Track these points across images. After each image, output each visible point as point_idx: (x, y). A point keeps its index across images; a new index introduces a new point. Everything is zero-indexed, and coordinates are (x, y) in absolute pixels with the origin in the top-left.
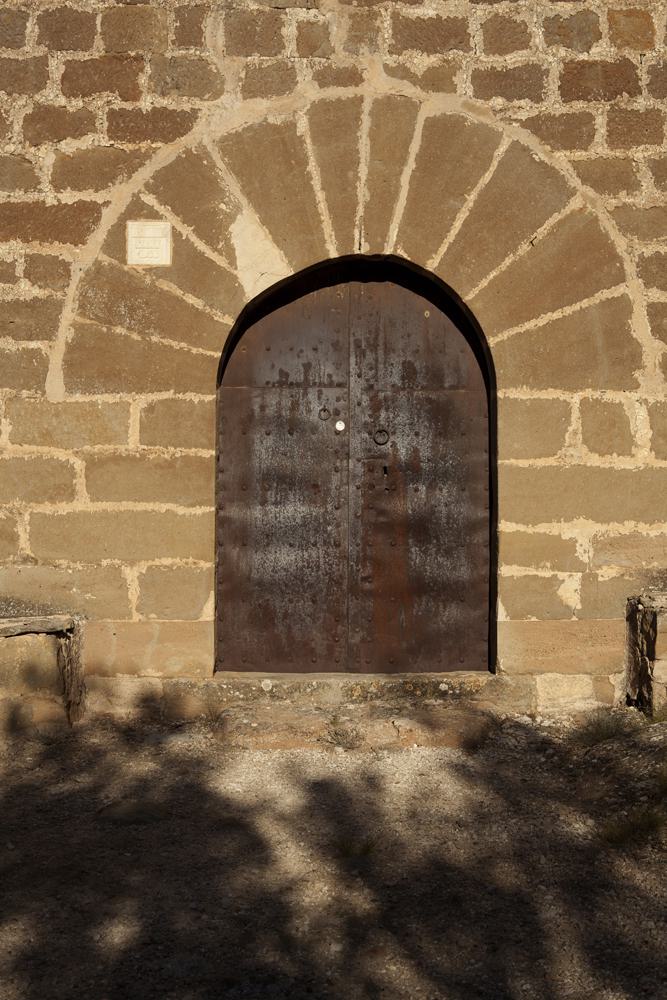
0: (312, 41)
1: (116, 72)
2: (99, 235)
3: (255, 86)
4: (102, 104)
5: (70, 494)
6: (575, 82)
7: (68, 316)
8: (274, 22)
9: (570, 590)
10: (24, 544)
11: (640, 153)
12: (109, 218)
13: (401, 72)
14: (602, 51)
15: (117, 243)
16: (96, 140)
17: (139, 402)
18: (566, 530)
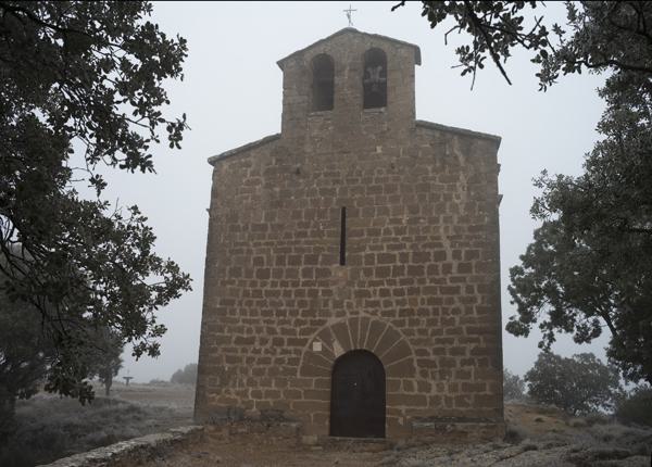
0: (350, 305)
1: (311, 313)
2: (308, 345)
3: (338, 315)
4: (309, 318)
5: (300, 397)
6: (402, 313)
7: (301, 361)
8: (342, 302)
9: (401, 421)
10: (292, 408)
11: (415, 328)
12: (310, 341)
13: (367, 312)
14: (407, 307)
15: (311, 346)
16: (308, 325)
17: (314, 379)
18: (398, 407)
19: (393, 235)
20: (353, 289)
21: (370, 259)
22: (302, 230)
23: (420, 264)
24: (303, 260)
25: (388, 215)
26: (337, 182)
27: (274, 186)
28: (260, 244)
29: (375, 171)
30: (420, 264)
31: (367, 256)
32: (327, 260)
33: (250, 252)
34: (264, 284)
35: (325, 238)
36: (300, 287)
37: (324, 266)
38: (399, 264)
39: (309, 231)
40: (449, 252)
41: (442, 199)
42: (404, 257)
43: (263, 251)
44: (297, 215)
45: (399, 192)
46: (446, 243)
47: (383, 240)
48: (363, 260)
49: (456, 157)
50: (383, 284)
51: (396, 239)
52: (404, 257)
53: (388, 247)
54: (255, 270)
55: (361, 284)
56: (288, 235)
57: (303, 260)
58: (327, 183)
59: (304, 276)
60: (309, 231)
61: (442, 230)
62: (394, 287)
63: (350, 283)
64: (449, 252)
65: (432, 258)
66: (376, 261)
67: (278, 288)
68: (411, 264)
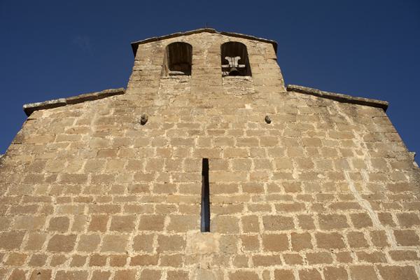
19: (283, 193)
20: (226, 271)
21: (251, 223)
22: (143, 183)
23: (334, 231)
24: (137, 223)
25: (272, 169)
26: (197, 132)
27: (107, 134)
28: (69, 200)
29: (246, 125)
30: (334, 231)
31: (245, 219)
32: (178, 225)
33: (48, 210)
34: (58, 261)
35: (177, 194)
36: (127, 267)
37: (173, 233)
38: (300, 231)
39: (151, 185)
40: (374, 216)
41: (339, 154)
42: (306, 222)
43: (70, 209)
44: (136, 165)
45: (280, 145)
46: (366, 206)
47: (269, 198)
48: (240, 224)
49: (342, 118)
50: (280, 263)
51: (288, 198)
52: (306, 222)
53: (279, 208)
54: (49, 237)
55: (241, 261)
56: (118, 189)
57: (137, 223)
58: (182, 133)
59: (136, 248)
60: (151, 185)
61: (352, 187)
62: (299, 267)
63: (221, 260)
64: (374, 216)
65: (349, 221)
66: (262, 226)
67: (85, 267)
68: (319, 230)
